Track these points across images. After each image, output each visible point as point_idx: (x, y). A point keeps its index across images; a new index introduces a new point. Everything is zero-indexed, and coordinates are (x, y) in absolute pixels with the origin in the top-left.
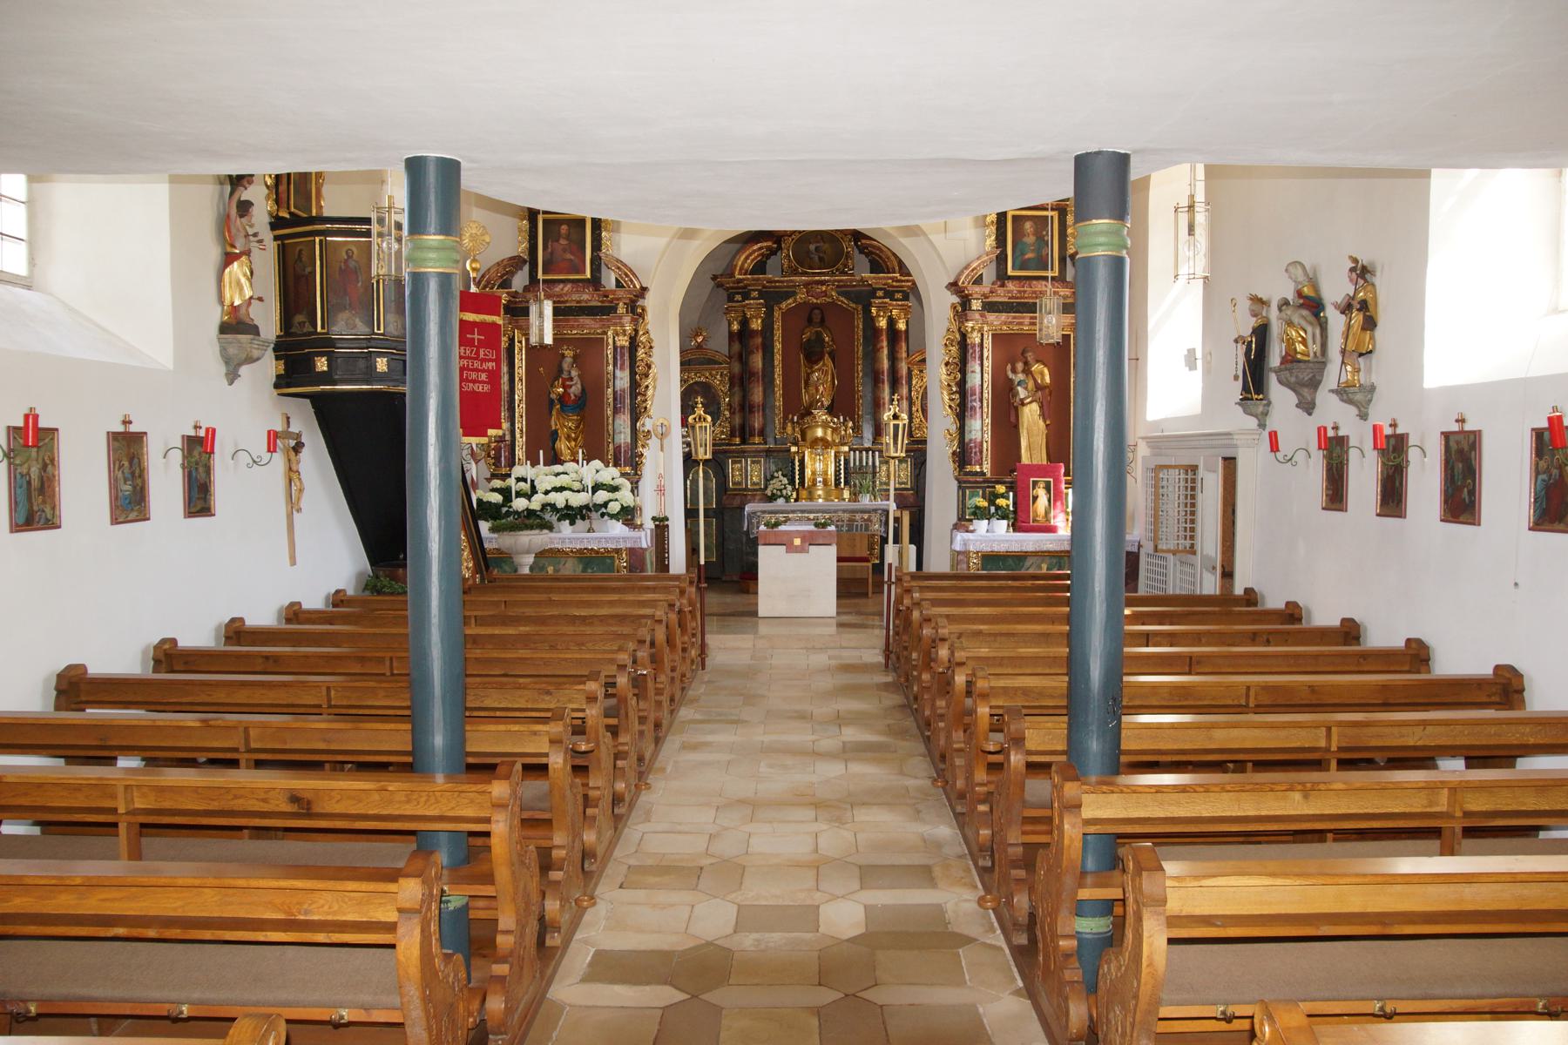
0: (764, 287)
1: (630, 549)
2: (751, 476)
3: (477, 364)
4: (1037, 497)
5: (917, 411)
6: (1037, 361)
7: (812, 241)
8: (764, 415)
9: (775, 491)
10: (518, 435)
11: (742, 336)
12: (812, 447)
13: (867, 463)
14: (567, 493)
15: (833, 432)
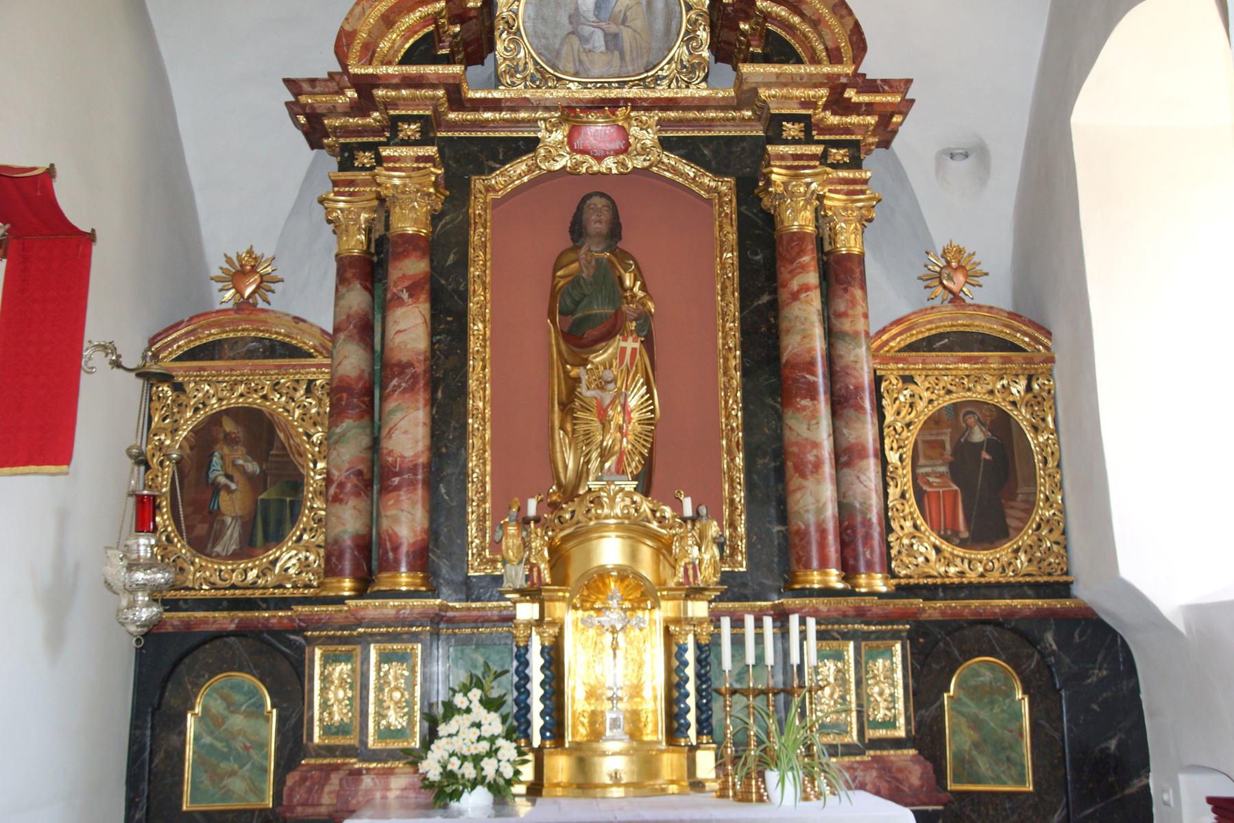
2: (380, 702)
5: (903, 496)
8: (434, 508)
9: (454, 764)
12: (585, 604)
13: (760, 658)
15: (657, 552)
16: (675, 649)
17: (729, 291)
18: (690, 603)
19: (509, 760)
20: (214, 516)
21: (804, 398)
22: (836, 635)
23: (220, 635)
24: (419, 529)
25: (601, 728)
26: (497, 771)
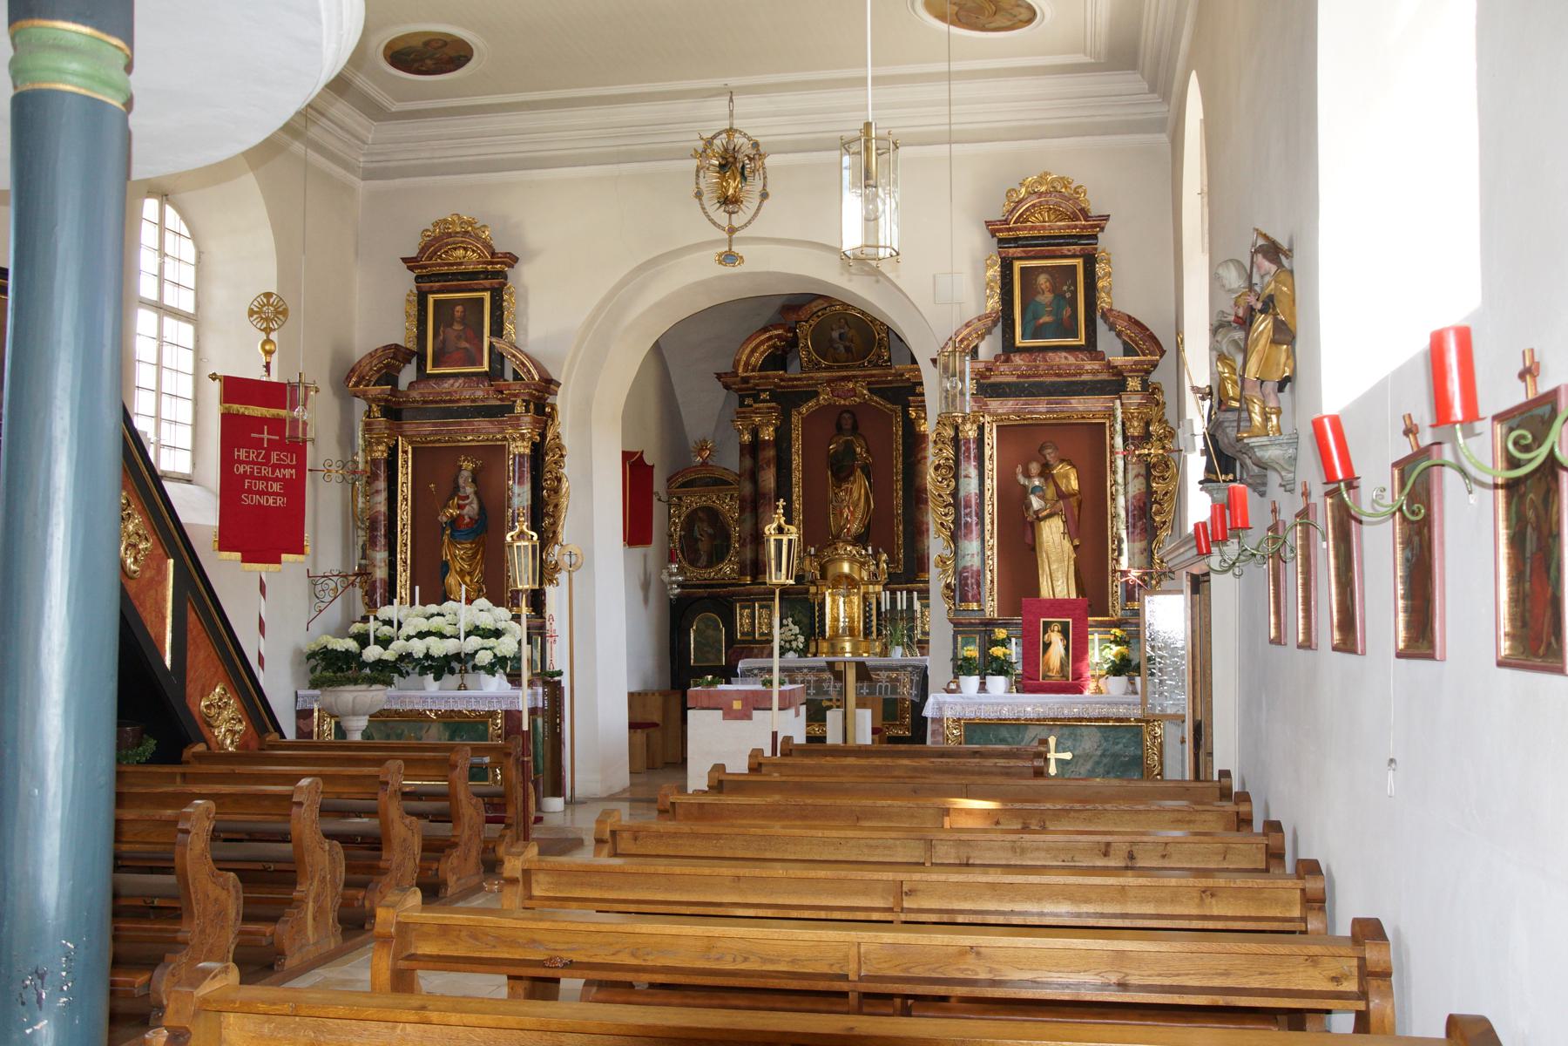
0: (777, 386)
1: (506, 711)
2: (760, 623)
3: (266, 471)
4: (1050, 644)
6: (1062, 461)
7: (834, 326)
10: (399, 568)
11: (753, 449)
14: (431, 640)
15: (861, 567)
20: (697, 551)
23: (701, 598)
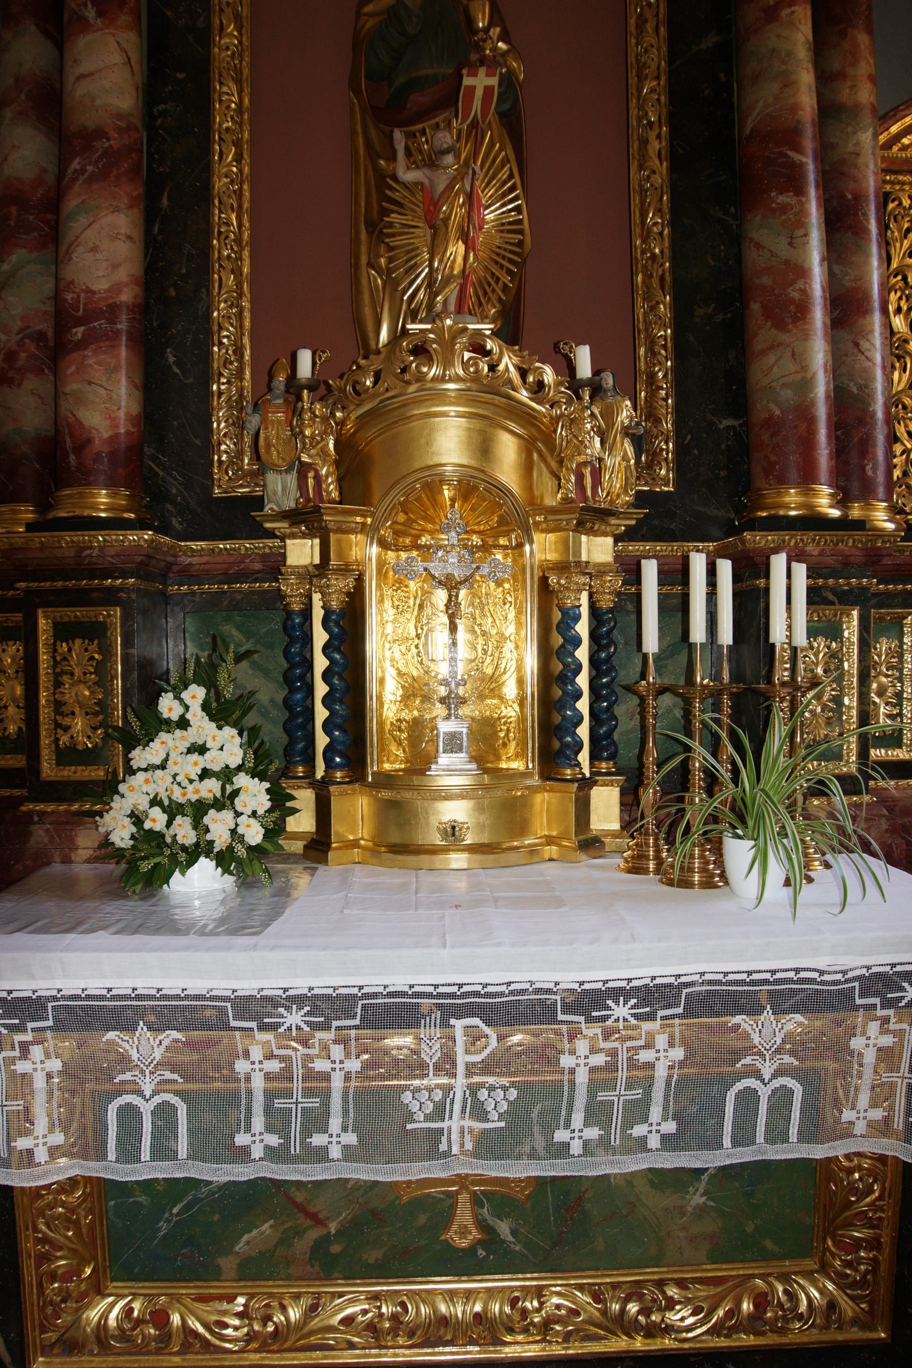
2: (58, 706)
9: (157, 820)
15: (528, 447)
16: (557, 616)
17: (649, 27)
18: (584, 538)
19: (254, 814)
21: (782, 191)
22: (831, 597)
24: (122, 414)
25: (431, 748)
26: (233, 832)
